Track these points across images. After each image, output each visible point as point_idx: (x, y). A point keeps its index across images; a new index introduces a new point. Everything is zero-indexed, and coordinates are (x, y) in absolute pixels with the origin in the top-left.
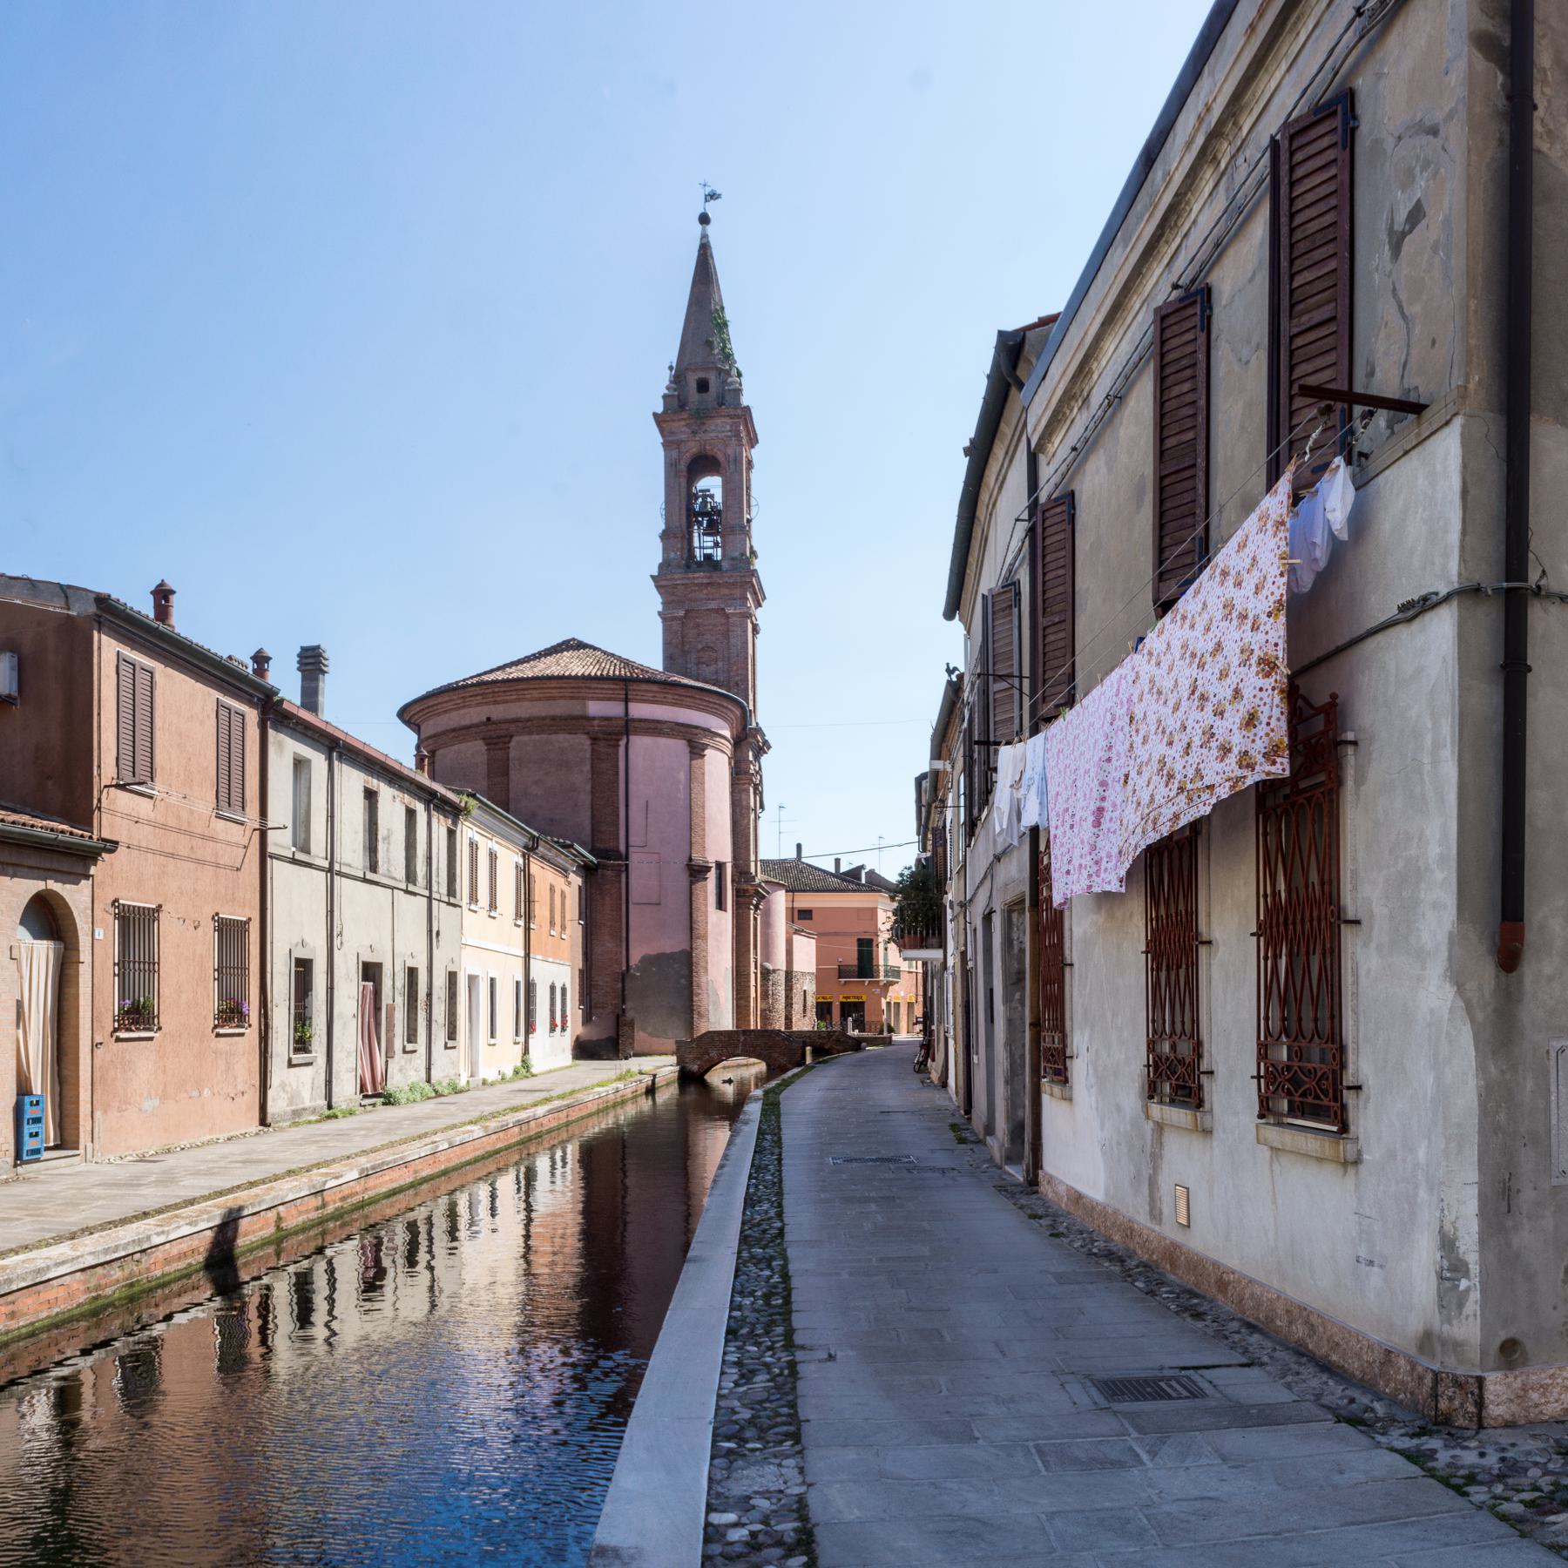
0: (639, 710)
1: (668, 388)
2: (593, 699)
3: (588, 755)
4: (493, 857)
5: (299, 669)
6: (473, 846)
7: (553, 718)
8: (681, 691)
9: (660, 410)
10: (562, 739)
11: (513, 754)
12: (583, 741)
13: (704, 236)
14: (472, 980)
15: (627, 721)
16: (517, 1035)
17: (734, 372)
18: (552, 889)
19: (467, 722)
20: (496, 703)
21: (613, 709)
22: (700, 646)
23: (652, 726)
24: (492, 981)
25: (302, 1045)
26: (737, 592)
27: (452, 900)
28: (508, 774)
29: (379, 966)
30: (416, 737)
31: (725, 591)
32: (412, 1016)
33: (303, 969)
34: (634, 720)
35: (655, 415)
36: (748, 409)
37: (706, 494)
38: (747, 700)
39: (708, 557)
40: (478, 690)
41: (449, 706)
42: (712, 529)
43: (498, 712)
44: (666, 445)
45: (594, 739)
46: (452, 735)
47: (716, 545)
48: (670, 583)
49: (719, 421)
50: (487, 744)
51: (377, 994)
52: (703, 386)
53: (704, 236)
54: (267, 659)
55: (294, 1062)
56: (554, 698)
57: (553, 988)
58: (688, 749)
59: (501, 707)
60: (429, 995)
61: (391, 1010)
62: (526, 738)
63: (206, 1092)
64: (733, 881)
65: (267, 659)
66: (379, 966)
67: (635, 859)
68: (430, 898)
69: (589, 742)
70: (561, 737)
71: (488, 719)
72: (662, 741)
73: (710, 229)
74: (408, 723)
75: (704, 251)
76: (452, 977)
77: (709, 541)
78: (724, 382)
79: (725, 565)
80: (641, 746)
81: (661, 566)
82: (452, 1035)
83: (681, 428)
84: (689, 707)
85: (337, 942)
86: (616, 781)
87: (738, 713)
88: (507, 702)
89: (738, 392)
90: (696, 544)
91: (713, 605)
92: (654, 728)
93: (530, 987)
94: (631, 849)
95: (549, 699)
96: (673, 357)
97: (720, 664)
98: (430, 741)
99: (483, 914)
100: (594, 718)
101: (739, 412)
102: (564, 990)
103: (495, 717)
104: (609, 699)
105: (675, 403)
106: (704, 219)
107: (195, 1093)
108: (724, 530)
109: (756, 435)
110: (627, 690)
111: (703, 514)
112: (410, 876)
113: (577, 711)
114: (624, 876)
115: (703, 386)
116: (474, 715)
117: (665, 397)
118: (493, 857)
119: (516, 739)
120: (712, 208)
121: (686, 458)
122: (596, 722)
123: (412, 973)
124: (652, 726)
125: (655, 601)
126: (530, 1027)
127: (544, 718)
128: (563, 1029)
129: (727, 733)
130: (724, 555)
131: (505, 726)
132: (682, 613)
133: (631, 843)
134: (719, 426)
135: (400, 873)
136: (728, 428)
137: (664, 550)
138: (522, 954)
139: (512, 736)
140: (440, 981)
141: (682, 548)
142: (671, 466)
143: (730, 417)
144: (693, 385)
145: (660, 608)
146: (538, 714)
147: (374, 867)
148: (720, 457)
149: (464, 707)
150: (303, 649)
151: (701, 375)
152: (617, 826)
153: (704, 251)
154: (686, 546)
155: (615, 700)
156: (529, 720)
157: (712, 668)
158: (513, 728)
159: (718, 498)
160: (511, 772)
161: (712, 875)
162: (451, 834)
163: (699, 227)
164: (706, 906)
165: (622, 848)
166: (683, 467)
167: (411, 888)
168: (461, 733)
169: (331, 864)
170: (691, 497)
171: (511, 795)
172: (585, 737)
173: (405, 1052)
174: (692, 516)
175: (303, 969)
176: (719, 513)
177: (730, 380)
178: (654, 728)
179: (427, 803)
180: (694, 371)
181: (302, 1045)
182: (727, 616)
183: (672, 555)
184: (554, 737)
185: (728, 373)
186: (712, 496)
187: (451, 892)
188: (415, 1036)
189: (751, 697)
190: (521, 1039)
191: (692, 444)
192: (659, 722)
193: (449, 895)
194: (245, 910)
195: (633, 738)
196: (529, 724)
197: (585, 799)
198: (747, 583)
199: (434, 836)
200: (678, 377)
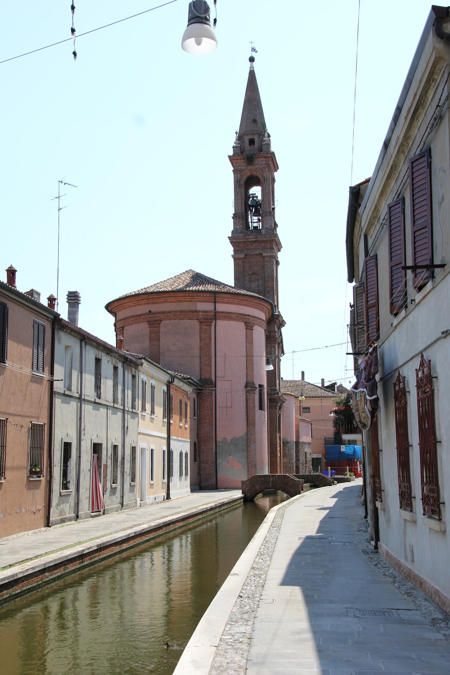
0: (221, 307)
1: (235, 143)
2: (199, 301)
3: (198, 330)
4: (153, 387)
5: (67, 302)
6: (144, 383)
7: (181, 312)
8: (241, 298)
9: (231, 154)
10: (186, 323)
11: (162, 329)
12: (196, 323)
13: (252, 67)
14: (143, 450)
15: (215, 313)
16: (164, 479)
17: (266, 135)
18: (181, 402)
19: (139, 313)
20: (154, 303)
21: (209, 307)
22: (250, 273)
23: (227, 315)
24: (152, 450)
25: (65, 486)
26: (268, 245)
27: (134, 411)
28: (159, 340)
29: (100, 445)
30: (114, 319)
31: (263, 245)
32: (115, 470)
33: (67, 446)
34: (218, 312)
35: (229, 157)
36: (273, 153)
37: (254, 196)
38: (274, 302)
39: (256, 228)
40: (145, 297)
41: (131, 304)
42: (257, 213)
43: (154, 308)
44: (235, 172)
45: (201, 322)
46: (132, 319)
47: (259, 220)
48: (237, 241)
49: (259, 160)
50: (149, 325)
51: (99, 459)
52: (252, 142)
53: (252, 67)
54: (55, 299)
55: (62, 494)
56: (181, 301)
57: (181, 454)
58: (245, 327)
59: (156, 305)
60: (123, 458)
61: (106, 466)
62: (168, 322)
63: (23, 510)
64: (268, 394)
65: (55, 299)
66: (100, 445)
67: (219, 384)
68: (124, 410)
69: (199, 324)
70: (185, 321)
71: (150, 311)
72: (233, 323)
73: (254, 64)
74: (110, 312)
75: (252, 75)
76: (134, 449)
77: (255, 219)
78: (262, 141)
79: (263, 232)
80: (222, 324)
81: (233, 232)
82: (133, 480)
83: (242, 164)
84: (245, 305)
85: (83, 432)
86: (210, 344)
87: (269, 307)
88: (159, 303)
89: (269, 145)
90: (250, 220)
91: (257, 252)
92: (228, 316)
93: (170, 453)
94: (217, 379)
95: (179, 302)
96: (237, 128)
97: (260, 282)
98: (121, 322)
99: (148, 417)
100: (199, 311)
101: (269, 155)
102: (186, 454)
103: (153, 311)
104: (207, 302)
105: (239, 151)
106: (252, 60)
107: (19, 511)
108: (263, 213)
109: (278, 165)
110: (215, 297)
111: (253, 206)
112: (115, 400)
113: (193, 309)
114: (214, 392)
115: (252, 142)
116: (142, 309)
117: (234, 147)
118: (153, 387)
119: (163, 322)
120: (254, 55)
121: (245, 178)
122: (200, 314)
123: (115, 447)
124: (227, 315)
125: (230, 250)
126: (170, 474)
127: (176, 312)
128: (186, 474)
129: (264, 318)
130: (262, 226)
131: (158, 315)
132: (243, 256)
133: (217, 376)
134: (260, 162)
135: (110, 397)
136: (264, 163)
137: (235, 224)
138: (165, 436)
139: (161, 321)
140: (128, 452)
141: (243, 223)
142: (237, 183)
143: (265, 157)
144: (247, 142)
145: (233, 253)
146: (174, 310)
147: (99, 397)
148: (260, 177)
149: (138, 305)
150: (70, 293)
151: (251, 137)
152: (211, 366)
153: (252, 75)
154: (244, 223)
155: (210, 302)
156: (170, 312)
157: (256, 283)
158: (162, 316)
159: (260, 198)
160: (161, 339)
161: (257, 391)
162: (134, 377)
163: (249, 63)
164: (254, 407)
165: (213, 379)
166: (243, 182)
167: (116, 406)
168: (137, 318)
169: (81, 395)
170: (247, 196)
171: (161, 351)
172: (196, 321)
173: (111, 488)
174: (247, 207)
175: (67, 446)
176: (260, 205)
177: (264, 139)
178: (228, 316)
179: (124, 363)
180: (247, 135)
181: (65, 486)
182: (264, 257)
183: (238, 227)
184: (181, 321)
185: (264, 136)
186: (257, 197)
187: (133, 407)
188: (116, 480)
189: (276, 298)
190: (166, 480)
191: (247, 171)
192: (231, 313)
193: (132, 408)
194: (43, 421)
195: (217, 321)
196: (169, 314)
197: (196, 352)
198: (273, 240)
199: (126, 379)
200: (240, 137)
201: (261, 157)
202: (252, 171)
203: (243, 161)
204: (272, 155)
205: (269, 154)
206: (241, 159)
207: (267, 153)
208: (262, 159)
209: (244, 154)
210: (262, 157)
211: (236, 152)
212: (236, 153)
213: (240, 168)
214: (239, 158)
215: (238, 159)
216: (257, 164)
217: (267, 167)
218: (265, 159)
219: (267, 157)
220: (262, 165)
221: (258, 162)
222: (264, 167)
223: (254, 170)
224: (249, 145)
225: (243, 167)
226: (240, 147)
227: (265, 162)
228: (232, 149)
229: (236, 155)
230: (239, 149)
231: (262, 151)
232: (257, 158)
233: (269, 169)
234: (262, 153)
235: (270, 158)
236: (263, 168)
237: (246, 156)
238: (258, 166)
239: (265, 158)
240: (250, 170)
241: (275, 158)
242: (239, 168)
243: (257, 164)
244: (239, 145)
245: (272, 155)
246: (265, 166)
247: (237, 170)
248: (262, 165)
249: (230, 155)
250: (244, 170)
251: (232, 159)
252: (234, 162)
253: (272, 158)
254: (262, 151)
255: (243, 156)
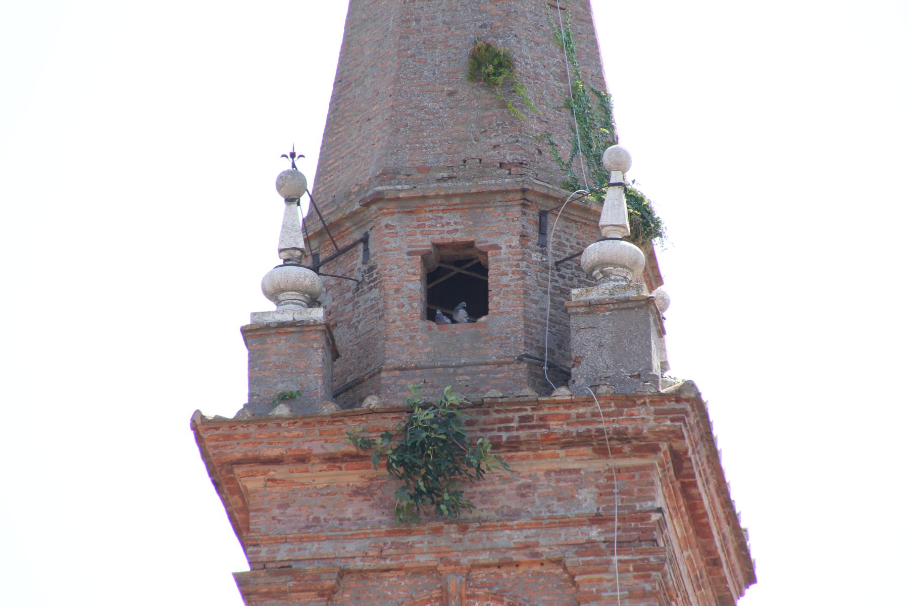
109: (740, 536)
201: (551, 441)
202: (454, 582)
203: (352, 477)
204: (679, 416)
205: (641, 412)
206: (332, 460)
207: (630, 400)
208: (568, 460)
209: (372, 402)
210: (568, 443)
211: (281, 387)
212: (285, 398)
213: (327, 549)
214: (317, 448)
215: (302, 459)
216: (515, 514)
217: (623, 546)
218: (600, 464)
219: (621, 436)
220: (565, 523)
221: (524, 491)
222: (589, 548)
223: (480, 576)
224: (430, 315)
225: (351, 547)
226: (328, 329)
227: (604, 493)
228: (240, 353)
229: (282, 410)
230: (318, 356)
231: (564, 377)
232: (514, 445)
233: (643, 570)
234: (562, 393)
235: (655, 449)
236: (572, 559)
237: (391, 424)
238: (519, 537)
239: (602, 452)
240: (431, 570)
241: (714, 456)
242: (311, 549)
243: (515, 514)
244: (318, 314)
245: (679, 416)
246: (594, 533)
247: (285, 569)
248: (565, 523)
249: (209, 414)
250: (362, 574)
251: (237, 451)
252: (253, 484)
253: (679, 459)
254: (564, 377)
255: (355, 426)
